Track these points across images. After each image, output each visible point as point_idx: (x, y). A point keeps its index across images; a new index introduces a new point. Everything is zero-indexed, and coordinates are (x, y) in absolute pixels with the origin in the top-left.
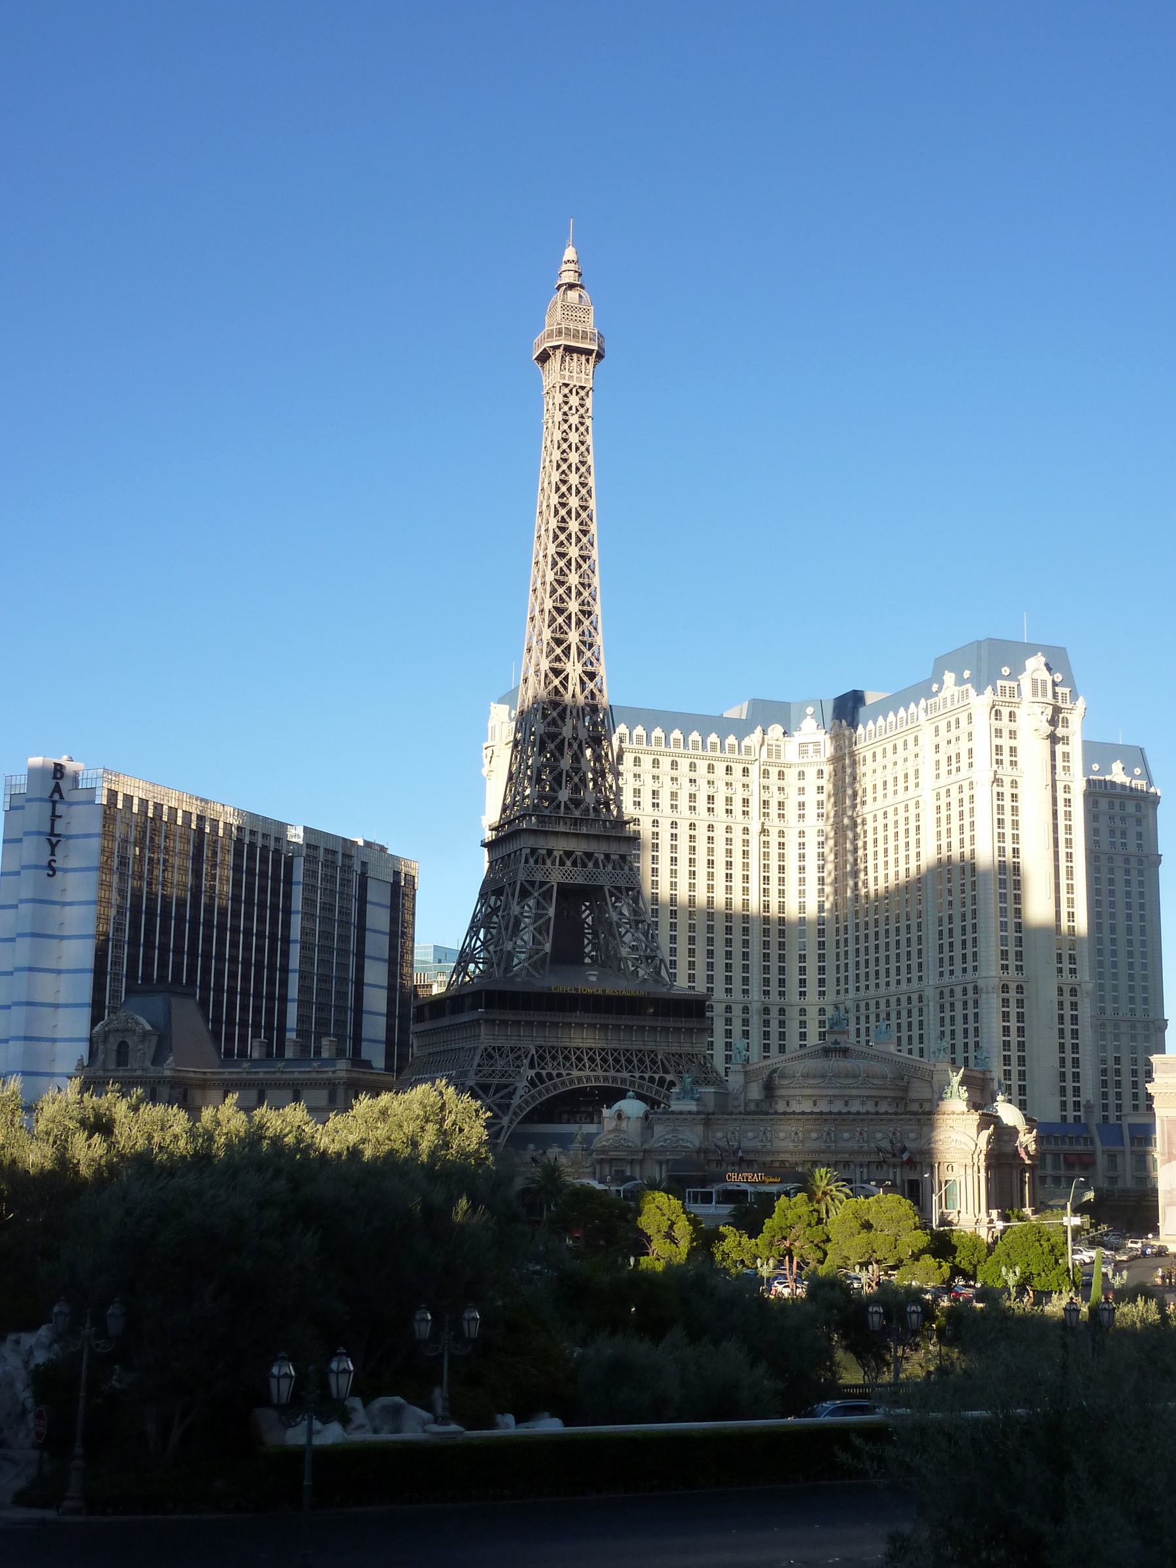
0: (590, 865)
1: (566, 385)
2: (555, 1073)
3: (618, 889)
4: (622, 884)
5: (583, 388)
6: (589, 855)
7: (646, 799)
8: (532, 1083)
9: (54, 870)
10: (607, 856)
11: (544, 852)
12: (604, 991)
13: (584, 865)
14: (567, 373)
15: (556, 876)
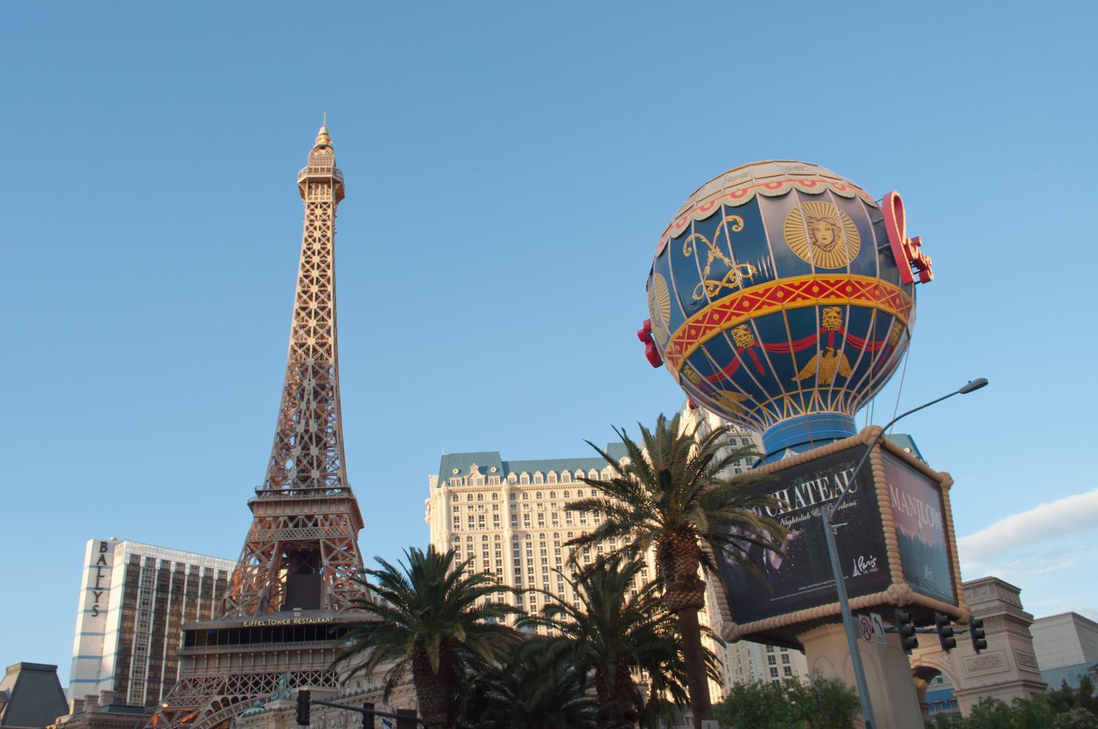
0: (310, 524)
1: (313, 203)
2: (230, 697)
3: (333, 541)
4: (336, 536)
5: (325, 203)
6: (310, 518)
7: (534, 519)
8: (216, 705)
9: (97, 612)
10: (326, 517)
11: (271, 519)
12: (292, 621)
13: (305, 525)
14: (313, 196)
15: (277, 535)
